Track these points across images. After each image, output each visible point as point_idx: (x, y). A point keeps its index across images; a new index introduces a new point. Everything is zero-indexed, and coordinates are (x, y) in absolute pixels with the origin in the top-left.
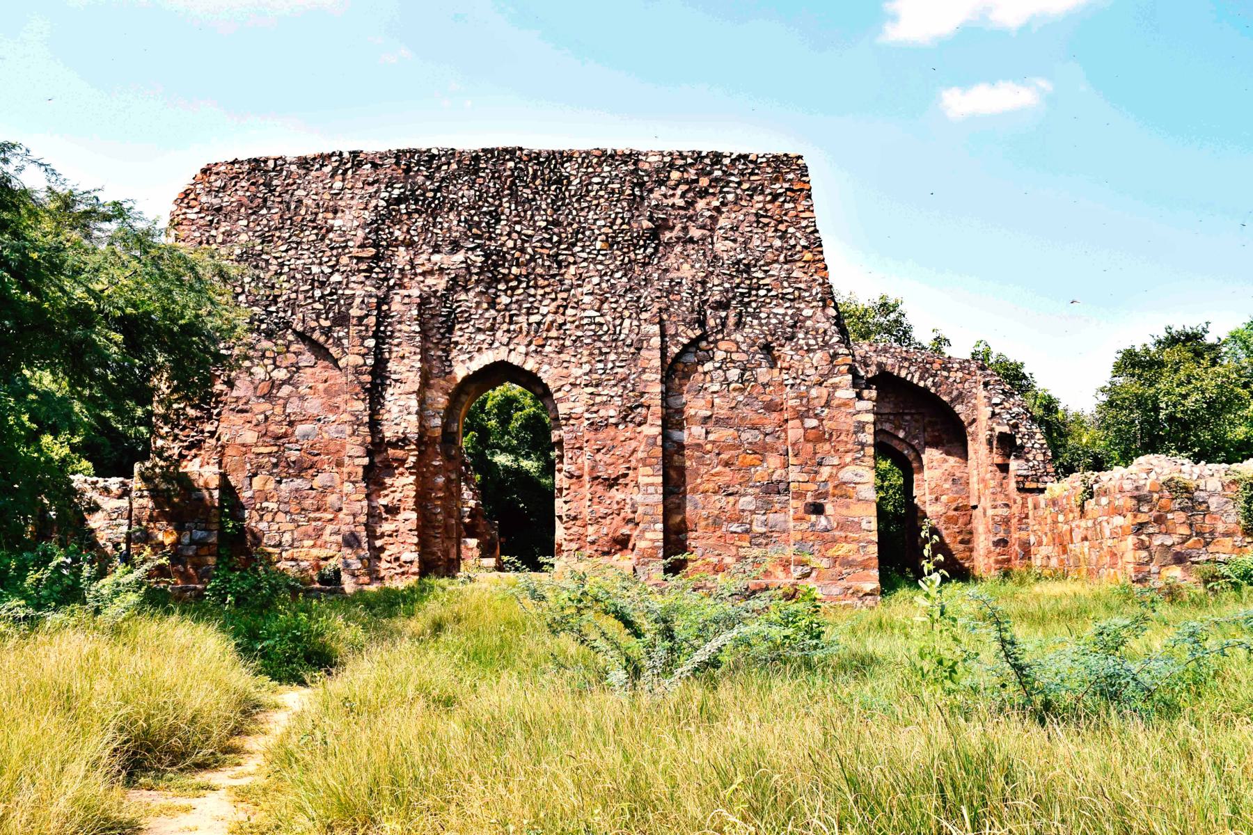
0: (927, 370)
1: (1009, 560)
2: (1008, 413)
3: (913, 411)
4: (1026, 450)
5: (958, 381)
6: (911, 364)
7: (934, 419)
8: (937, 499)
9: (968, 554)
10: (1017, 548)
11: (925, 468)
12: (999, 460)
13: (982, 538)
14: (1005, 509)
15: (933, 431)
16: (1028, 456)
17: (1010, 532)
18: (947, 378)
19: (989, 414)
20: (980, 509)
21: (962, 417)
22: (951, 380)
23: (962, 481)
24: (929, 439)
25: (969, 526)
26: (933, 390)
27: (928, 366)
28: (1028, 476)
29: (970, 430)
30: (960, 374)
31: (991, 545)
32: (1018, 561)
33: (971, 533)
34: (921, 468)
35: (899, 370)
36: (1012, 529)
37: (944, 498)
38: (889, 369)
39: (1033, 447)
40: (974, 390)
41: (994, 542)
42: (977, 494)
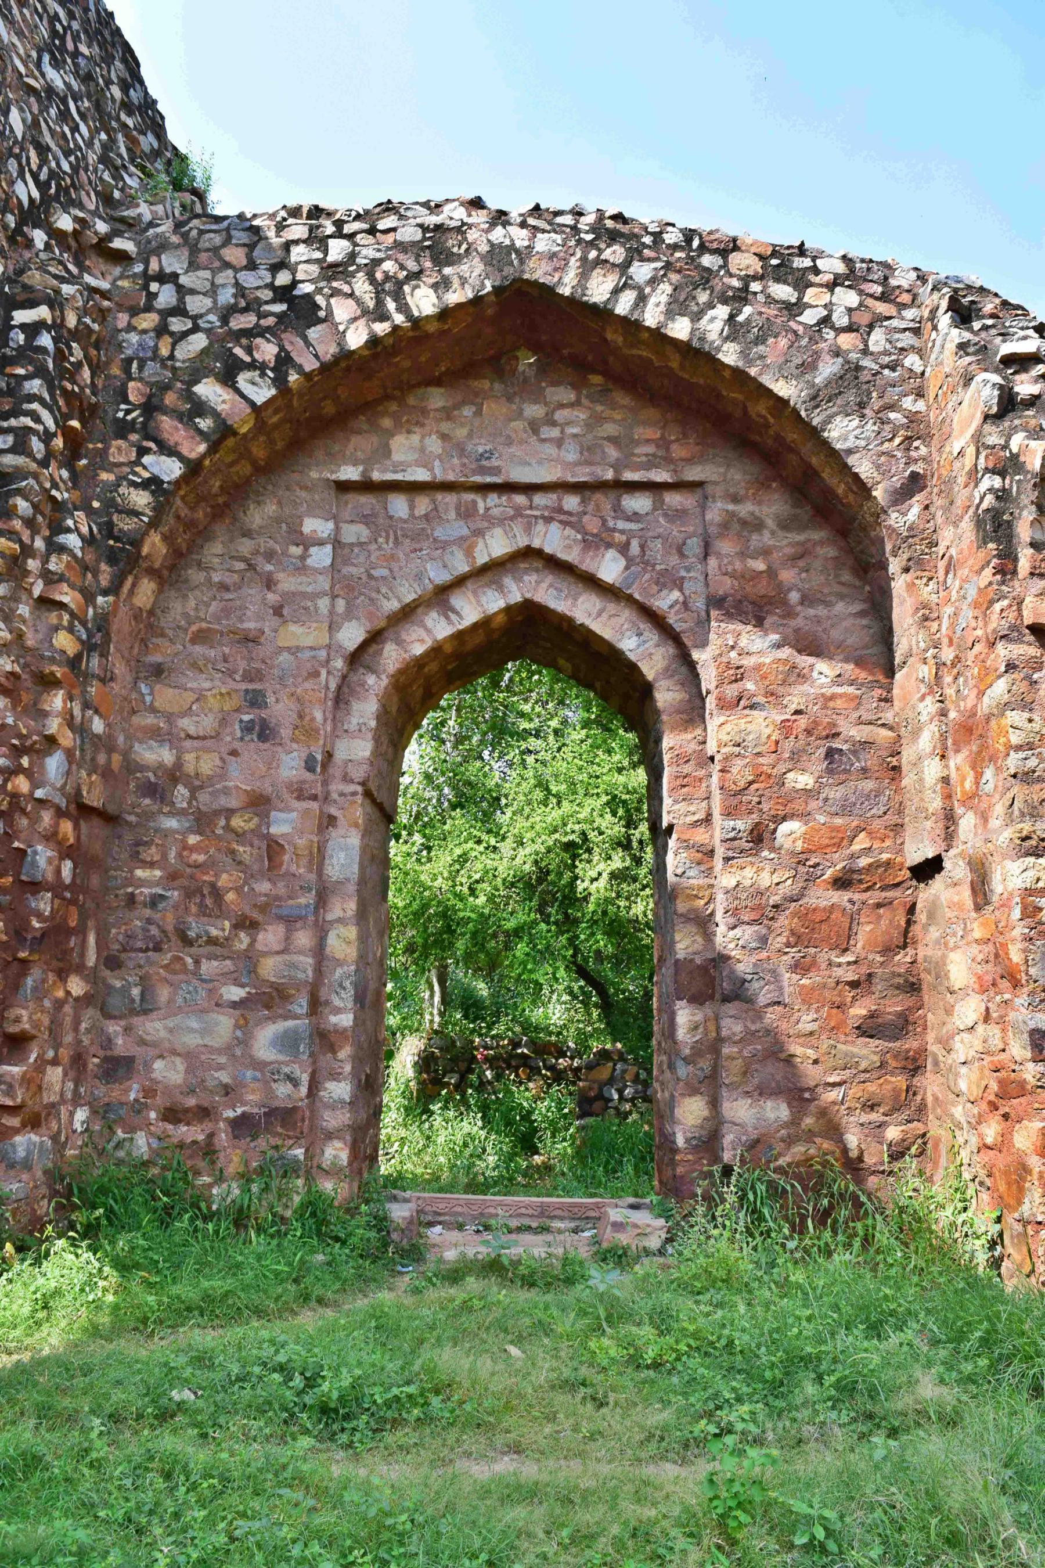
0: (706, 277)
3: (661, 476)
5: (840, 319)
6: (635, 254)
9: (899, 1081)
11: (710, 703)
13: (969, 1010)
15: (743, 555)
18: (794, 309)
20: (955, 867)
21: (863, 467)
22: (810, 317)
23: (868, 759)
24: (725, 585)
25: (903, 958)
26: (730, 355)
27: (707, 260)
30: (846, 297)
31: (1019, 1049)
33: (913, 987)
35: (584, 275)
38: (538, 272)
40: (912, 361)
42: (936, 804)
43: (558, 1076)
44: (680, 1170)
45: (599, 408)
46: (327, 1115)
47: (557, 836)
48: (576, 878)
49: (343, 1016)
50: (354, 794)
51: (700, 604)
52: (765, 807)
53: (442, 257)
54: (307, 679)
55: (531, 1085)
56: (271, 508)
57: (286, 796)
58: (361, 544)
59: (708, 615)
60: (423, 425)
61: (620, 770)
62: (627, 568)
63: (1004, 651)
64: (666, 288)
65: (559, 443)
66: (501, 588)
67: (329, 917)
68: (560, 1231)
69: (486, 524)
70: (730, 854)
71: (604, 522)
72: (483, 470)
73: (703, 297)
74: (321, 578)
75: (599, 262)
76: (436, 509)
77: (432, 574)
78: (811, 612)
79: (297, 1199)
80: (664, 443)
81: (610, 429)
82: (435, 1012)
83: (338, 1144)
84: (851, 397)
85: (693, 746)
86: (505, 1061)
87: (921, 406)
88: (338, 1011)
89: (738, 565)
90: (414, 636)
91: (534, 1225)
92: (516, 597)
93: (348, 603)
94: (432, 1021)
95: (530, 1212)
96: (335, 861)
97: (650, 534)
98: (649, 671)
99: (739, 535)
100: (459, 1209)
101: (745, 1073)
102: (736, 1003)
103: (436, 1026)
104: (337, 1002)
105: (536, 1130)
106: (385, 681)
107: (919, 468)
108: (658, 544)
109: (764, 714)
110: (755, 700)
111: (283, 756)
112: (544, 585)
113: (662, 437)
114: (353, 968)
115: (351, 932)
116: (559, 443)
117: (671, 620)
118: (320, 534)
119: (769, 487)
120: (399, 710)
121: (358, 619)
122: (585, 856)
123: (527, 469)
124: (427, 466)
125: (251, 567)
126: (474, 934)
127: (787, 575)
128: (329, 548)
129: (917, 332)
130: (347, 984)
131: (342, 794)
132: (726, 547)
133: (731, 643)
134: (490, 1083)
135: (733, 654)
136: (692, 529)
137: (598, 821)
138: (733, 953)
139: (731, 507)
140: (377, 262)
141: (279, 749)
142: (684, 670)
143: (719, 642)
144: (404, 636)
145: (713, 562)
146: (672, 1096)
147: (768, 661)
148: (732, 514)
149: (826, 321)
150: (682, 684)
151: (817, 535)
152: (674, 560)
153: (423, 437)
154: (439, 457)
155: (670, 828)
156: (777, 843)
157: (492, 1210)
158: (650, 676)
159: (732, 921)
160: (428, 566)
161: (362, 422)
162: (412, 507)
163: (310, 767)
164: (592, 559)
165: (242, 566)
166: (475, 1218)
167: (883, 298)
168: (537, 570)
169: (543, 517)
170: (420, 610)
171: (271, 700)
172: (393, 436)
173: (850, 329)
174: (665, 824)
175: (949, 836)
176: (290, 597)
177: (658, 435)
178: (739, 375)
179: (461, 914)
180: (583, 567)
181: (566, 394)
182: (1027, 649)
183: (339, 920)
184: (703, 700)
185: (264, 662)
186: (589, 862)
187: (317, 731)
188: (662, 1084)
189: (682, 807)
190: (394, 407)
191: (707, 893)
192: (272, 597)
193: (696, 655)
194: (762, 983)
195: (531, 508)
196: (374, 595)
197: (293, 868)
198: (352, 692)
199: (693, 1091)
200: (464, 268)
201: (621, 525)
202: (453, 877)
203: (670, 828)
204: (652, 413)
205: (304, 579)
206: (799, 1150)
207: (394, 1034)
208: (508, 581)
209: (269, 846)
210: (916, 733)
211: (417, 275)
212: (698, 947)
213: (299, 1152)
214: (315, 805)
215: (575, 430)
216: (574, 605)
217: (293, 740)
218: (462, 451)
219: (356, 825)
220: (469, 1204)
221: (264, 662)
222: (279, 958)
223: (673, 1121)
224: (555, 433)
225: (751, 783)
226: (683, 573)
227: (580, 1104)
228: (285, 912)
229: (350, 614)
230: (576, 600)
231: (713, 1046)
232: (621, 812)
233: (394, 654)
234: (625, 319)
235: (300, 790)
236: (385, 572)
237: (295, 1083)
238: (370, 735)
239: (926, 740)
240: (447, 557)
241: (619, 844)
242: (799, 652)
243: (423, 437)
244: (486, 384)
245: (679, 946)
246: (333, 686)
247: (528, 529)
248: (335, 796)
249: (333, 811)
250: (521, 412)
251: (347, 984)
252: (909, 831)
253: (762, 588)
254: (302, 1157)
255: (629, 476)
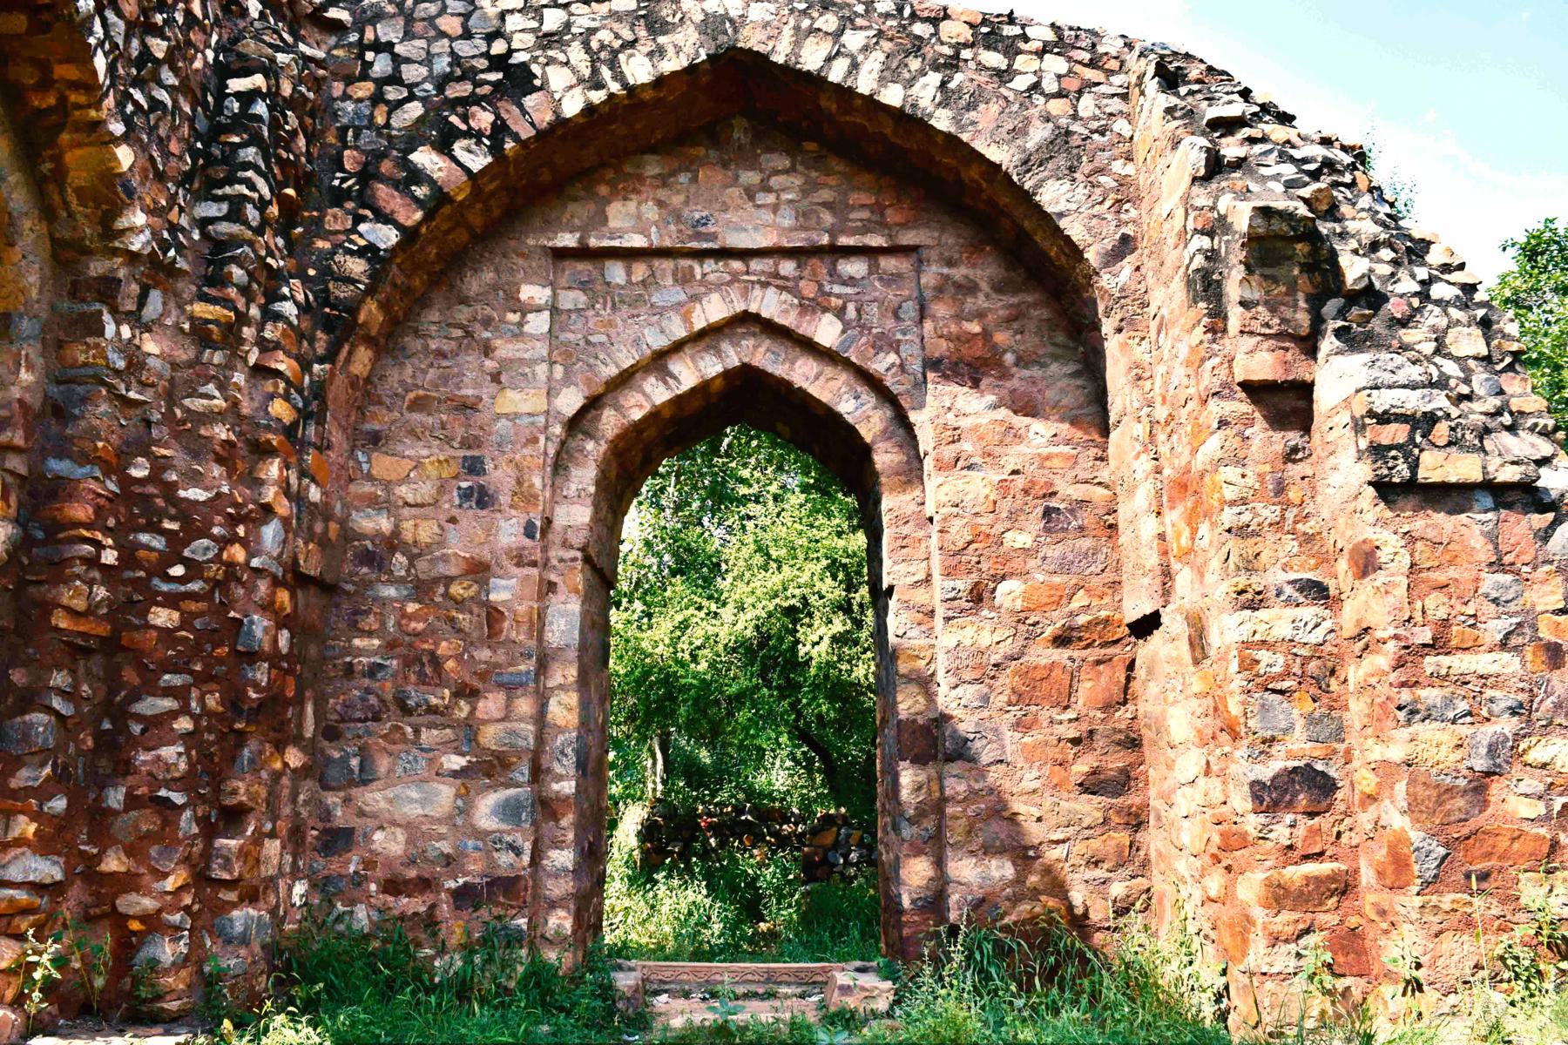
0: (918, 45)
1: (1344, 887)
2: (1284, 157)
3: (876, 241)
4: (1395, 308)
5: (1050, 85)
6: (848, 22)
7: (958, 273)
8: (978, 597)
9: (1123, 837)
10: (1398, 821)
11: (928, 464)
12: (1263, 364)
14: (1309, 612)
15: (959, 317)
16: (1408, 335)
17: (1339, 734)
18: (1004, 76)
19: (1198, 161)
20: (1173, 622)
21: (1074, 229)
22: (1020, 83)
23: (1086, 518)
24: (942, 348)
25: (1124, 715)
26: (942, 121)
27: (919, 29)
28: (1431, 419)
29: (1109, 281)
31: (1241, 801)
32: (1409, 901)
33: (1133, 743)
34: (912, 472)
36: (1356, 711)
37: (1009, 593)
38: (752, 39)
39: (1424, 296)
41: (1258, 790)
42: (1153, 560)
43: (783, 842)
44: (906, 932)
45: (814, 174)
46: (550, 883)
47: (777, 601)
48: (797, 642)
49: (565, 784)
50: (574, 560)
51: (916, 366)
52: (984, 566)
53: (657, 27)
54: (525, 445)
55: (755, 852)
56: (488, 276)
57: (506, 562)
58: (578, 310)
59: (925, 377)
60: (639, 192)
61: (839, 534)
62: (844, 332)
63: (1216, 408)
64: (878, 56)
65: (775, 209)
66: (719, 353)
67: (550, 684)
68: (787, 997)
69: (703, 289)
70: (950, 614)
71: (821, 286)
72: (698, 236)
73: (915, 64)
74: (539, 344)
75: (813, 31)
76: (653, 275)
77: (650, 340)
78: (1026, 373)
79: (520, 969)
80: (878, 209)
81: (826, 195)
82: (658, 780)
83: (561, 913)
84: (1062, 161)
85: (913, 507)
86: (728, 828)
87: (1130, 169)
88: (560, 778)
89: (953, 328)
90: (632, 402)
91: (761, 991)
92: (733, 360)
93: (566, 369)
94: (654, 790)
95: (756, 978)
96: (555, 627)
97: (867, 298)
98: (867, 432)
99: (954, 300)
100: (685, 977)
101: (969, 832)
102: (960, 763)
103: (658, 795)
104: (558, 769)
105: (761, 897)
106: (604, 447)
107: (1129, 230)
108: (874, 308)
109: (981, 474)
110: (973, 460)
111: (502, 523)
112: (762, 350)
113: (877, 202)
114: (574, 734)
115: (573, 699)
116: (775, 209)
117: (889, 382)
118: (538, 301)
119: (983, 250)
120: (618, 476)
121: (576, 385)
122: (807, 620)
123: (743, 235)
124: (644, 232)
125: (469, 334)
126: (696, 701)
127: (1001, 338)
128: (546, 314)
129: (1125, 97)
130: (569, 751)
131: (561, 560)
132: (941, 310)
133: (948, 404)
134: (714, 850)
135: (950, 416)
136: (906, 293)
137: (819, 584)
138: (955, 713)
139: (946, 271)
140: (592, 31)
141: (498, 515)
142: (901, 432)
143: (936, 404)
144: (622, 401)
145: (928, 325)
146: (897, 858)
147: (984, 421)
148: (947, 278)
149: (1036, 87)
150: (901, 447)
151: (1030, 299)
152: (890, 323)
153: (640, 203)
154: (656, 224)
155: (891, 589)
156: (997, 602)
157: (718, 977)
158: (868, 440)
159: (954, 680)
160: (646, 331)
161: (577, 189)
162: (629, 273)
163: (529, 531)
164: (809, 322)
165: (459, 333)
166: (700, 985)
167: (1092, 64)
168: (754, 335)
169: (759, 282)
170: (638, 375)
171: (489, 466)
172: (609, 202)
173: (1060, 94)
174: (885, 586)
175: (1166, 593)
176: (507, 363)
177: (873, 200)
178: (951, 140)
179: (683, 681)
180: (800, 331)
181: (784, 162)
182: (1240, 406)
183: (561, 687)
184: (921, 461)
185: (481, 428)
186: (810, 626)
187: (536, 497)
188: (887, 845)
189: (903, 568)
190: (610, 174)
191: (929, 654)
192: (490, 364)
193: (913, 417)
194: (984, 741)
195: (748, 273)
196: (592, 361)
197: (513, 634)
198: (571, 457)
199: (918, 852)
200: (678, 37)
201: (837, 289)
202: (674, 643)
203: (891, 589)
204: (866, 178)
205: (521, 345)
206: (1024, 908)
207: (617, 804)
208: (725, 346)
209: (488, 614)
210: (1131, 491)
211: (632, 44)
212: (921, 708)
213: (522, 922)
214: (534, 572)
215: (790, 197)
216: (792, 369)
217: (511, 506)
218: (678, 218)
219: (576, 591)
220: (694, 971)
221: (481, 428)
222: (500, 726)
223: (898, 882)
224: (771, 199)
225: (969, 543)
226: (899, 336)
227: (804, 870)
228: (505, 679)
229: (568, 380)
230: (793, 363)
231: (937, 806)
232: (841, 576)
233: (612, 419)
234: (838, 87)
235: (520, 556)
236: (604, 338)
237: (518, 852)
238: (589, 501)
239: (1142, 497)
240: (664, 323)
241: (840, 608)
242: (1015, 412)
243: (640, 203)
244: (702, 151)
245: (901, 707)
246: (552, 452)
247: (745, 294)
248: (554, 562)
249: (553, 577)
250: (737, 177)
251: (569, 751)
252: (1126, 588)
253: (978, 350)
254: (525, 927)
255: (844, 241)
